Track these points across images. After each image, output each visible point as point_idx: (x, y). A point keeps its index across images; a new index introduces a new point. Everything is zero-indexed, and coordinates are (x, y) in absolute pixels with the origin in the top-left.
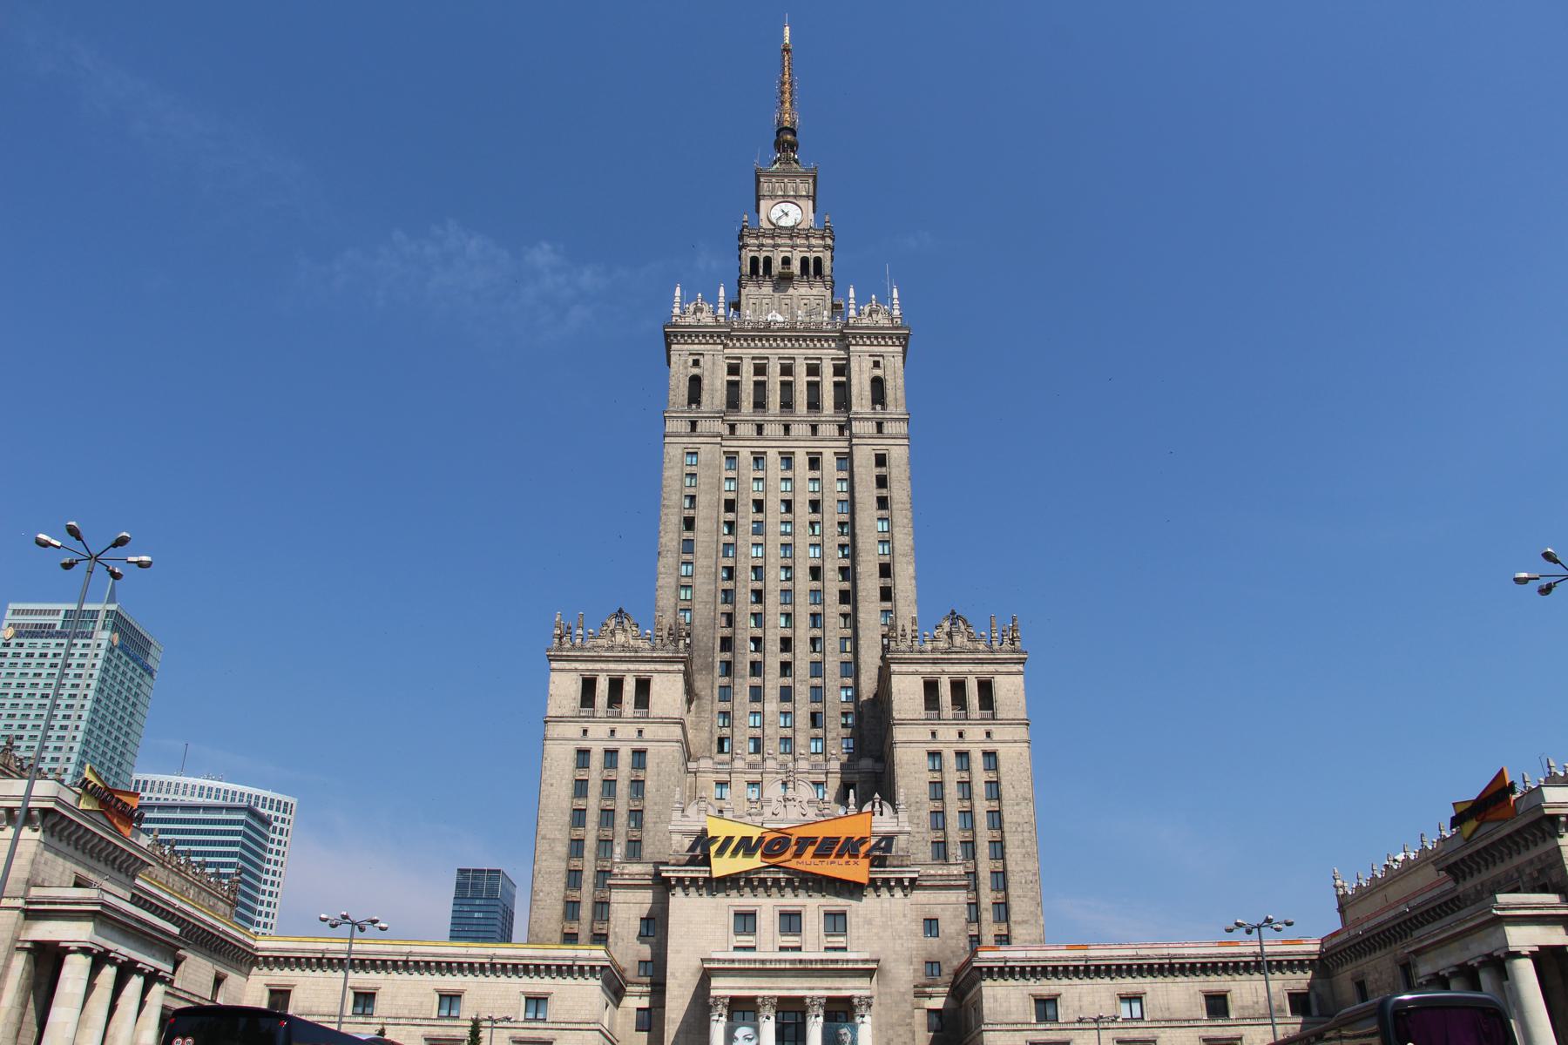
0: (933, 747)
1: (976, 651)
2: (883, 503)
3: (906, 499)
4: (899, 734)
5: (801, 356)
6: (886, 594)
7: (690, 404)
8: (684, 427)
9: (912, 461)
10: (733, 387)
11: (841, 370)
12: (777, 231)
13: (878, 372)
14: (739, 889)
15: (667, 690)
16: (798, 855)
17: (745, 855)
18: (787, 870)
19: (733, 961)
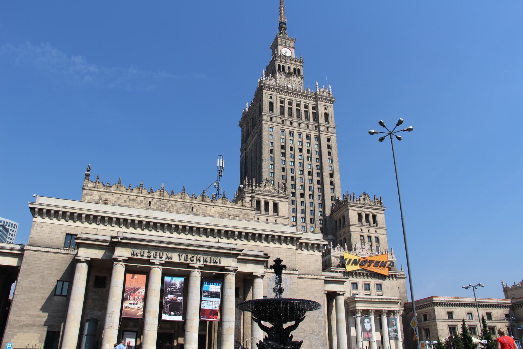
0: (362, 234)
1: (371, 205)
2: (329, 154)
3: (336, 154)
4: (352, 229)
5: (303, 101)
6: (332, 183)
7: (270, 111)
8: (269, 119)
9: (338, 141)
10: (282, 108)
11: (314, 108)
12: (285, 57)
13: (326, 111)
14: (352, 276)
15: (284, 207)
16: (369, 266)
17: (355, 265)
18: (366, 270)
19: (363, 298)
